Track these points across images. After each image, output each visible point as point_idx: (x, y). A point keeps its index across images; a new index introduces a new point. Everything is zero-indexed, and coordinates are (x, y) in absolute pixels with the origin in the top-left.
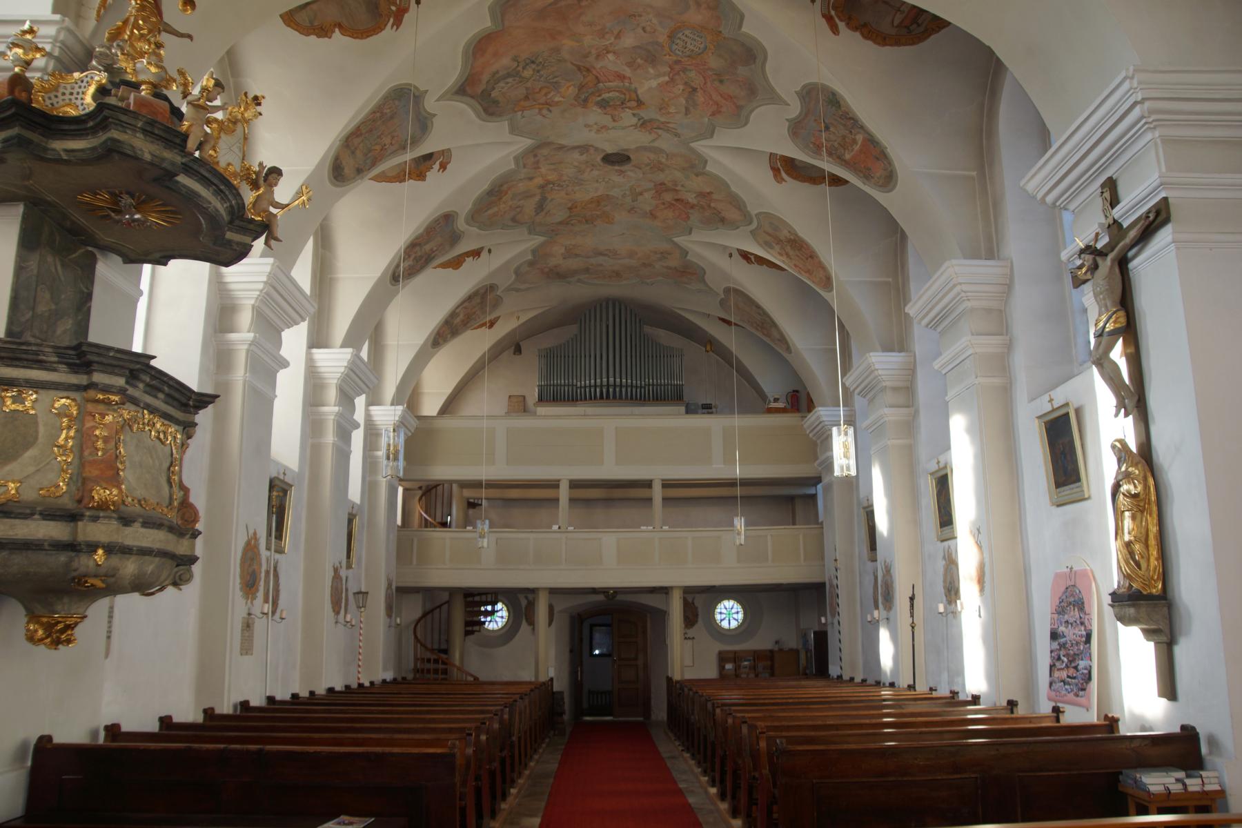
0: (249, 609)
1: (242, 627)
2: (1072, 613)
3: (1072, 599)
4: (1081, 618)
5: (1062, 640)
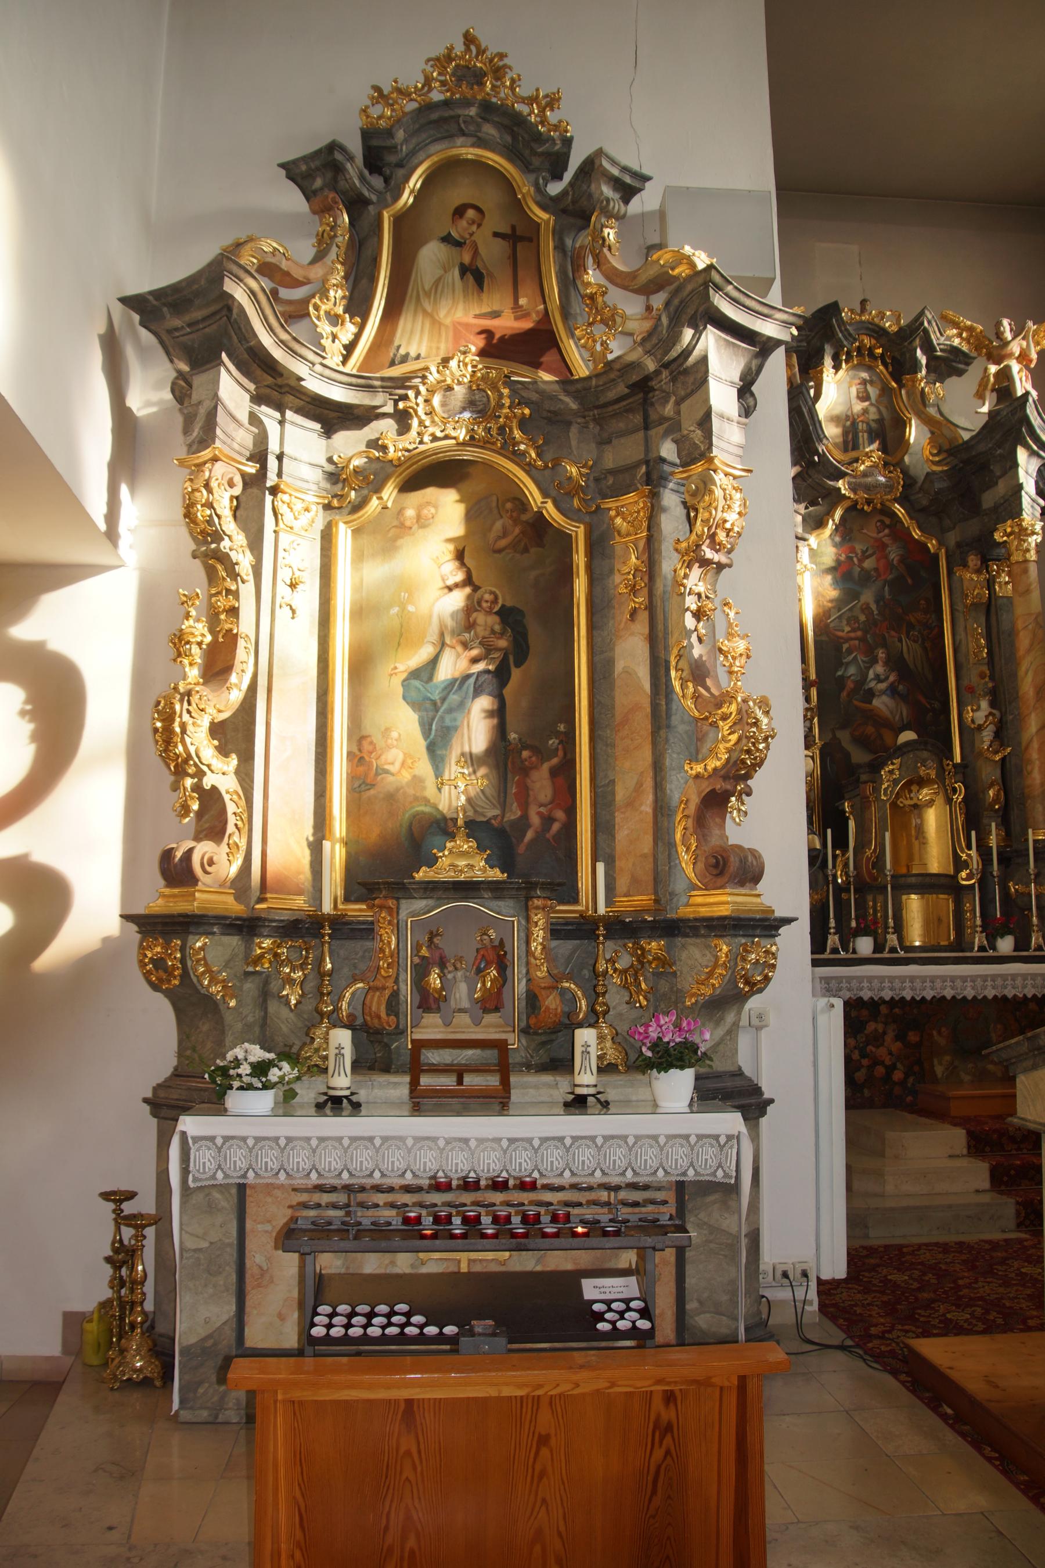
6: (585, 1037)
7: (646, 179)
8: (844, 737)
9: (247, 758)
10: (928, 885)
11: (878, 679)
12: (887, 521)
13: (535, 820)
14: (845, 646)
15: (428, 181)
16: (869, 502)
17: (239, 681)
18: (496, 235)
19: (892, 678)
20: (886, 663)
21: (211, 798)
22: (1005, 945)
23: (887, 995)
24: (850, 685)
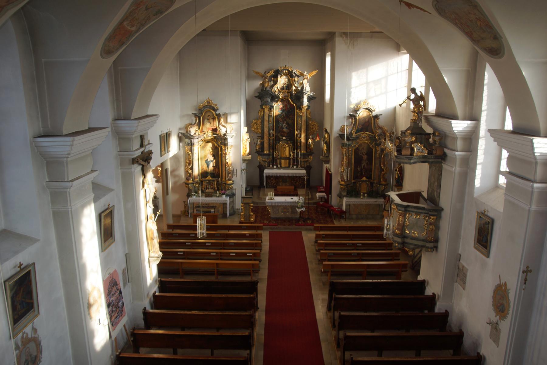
2: (114, 290)
4: (117, 288)
6: (218, 192)
7: (225, 113)
8: (279, 135)
10: (285, 159)
12: (288, 101)
13: (216, 172)
14: (280, 121)
15: (205, 113)
16: (285, 99)
17: (191, 164)
18: (212, 118)
19: (287, 126)
20: (286, 123)
21: (190, 174)
22: (295, 167)
23: (273, 175)
24: (280, 127)
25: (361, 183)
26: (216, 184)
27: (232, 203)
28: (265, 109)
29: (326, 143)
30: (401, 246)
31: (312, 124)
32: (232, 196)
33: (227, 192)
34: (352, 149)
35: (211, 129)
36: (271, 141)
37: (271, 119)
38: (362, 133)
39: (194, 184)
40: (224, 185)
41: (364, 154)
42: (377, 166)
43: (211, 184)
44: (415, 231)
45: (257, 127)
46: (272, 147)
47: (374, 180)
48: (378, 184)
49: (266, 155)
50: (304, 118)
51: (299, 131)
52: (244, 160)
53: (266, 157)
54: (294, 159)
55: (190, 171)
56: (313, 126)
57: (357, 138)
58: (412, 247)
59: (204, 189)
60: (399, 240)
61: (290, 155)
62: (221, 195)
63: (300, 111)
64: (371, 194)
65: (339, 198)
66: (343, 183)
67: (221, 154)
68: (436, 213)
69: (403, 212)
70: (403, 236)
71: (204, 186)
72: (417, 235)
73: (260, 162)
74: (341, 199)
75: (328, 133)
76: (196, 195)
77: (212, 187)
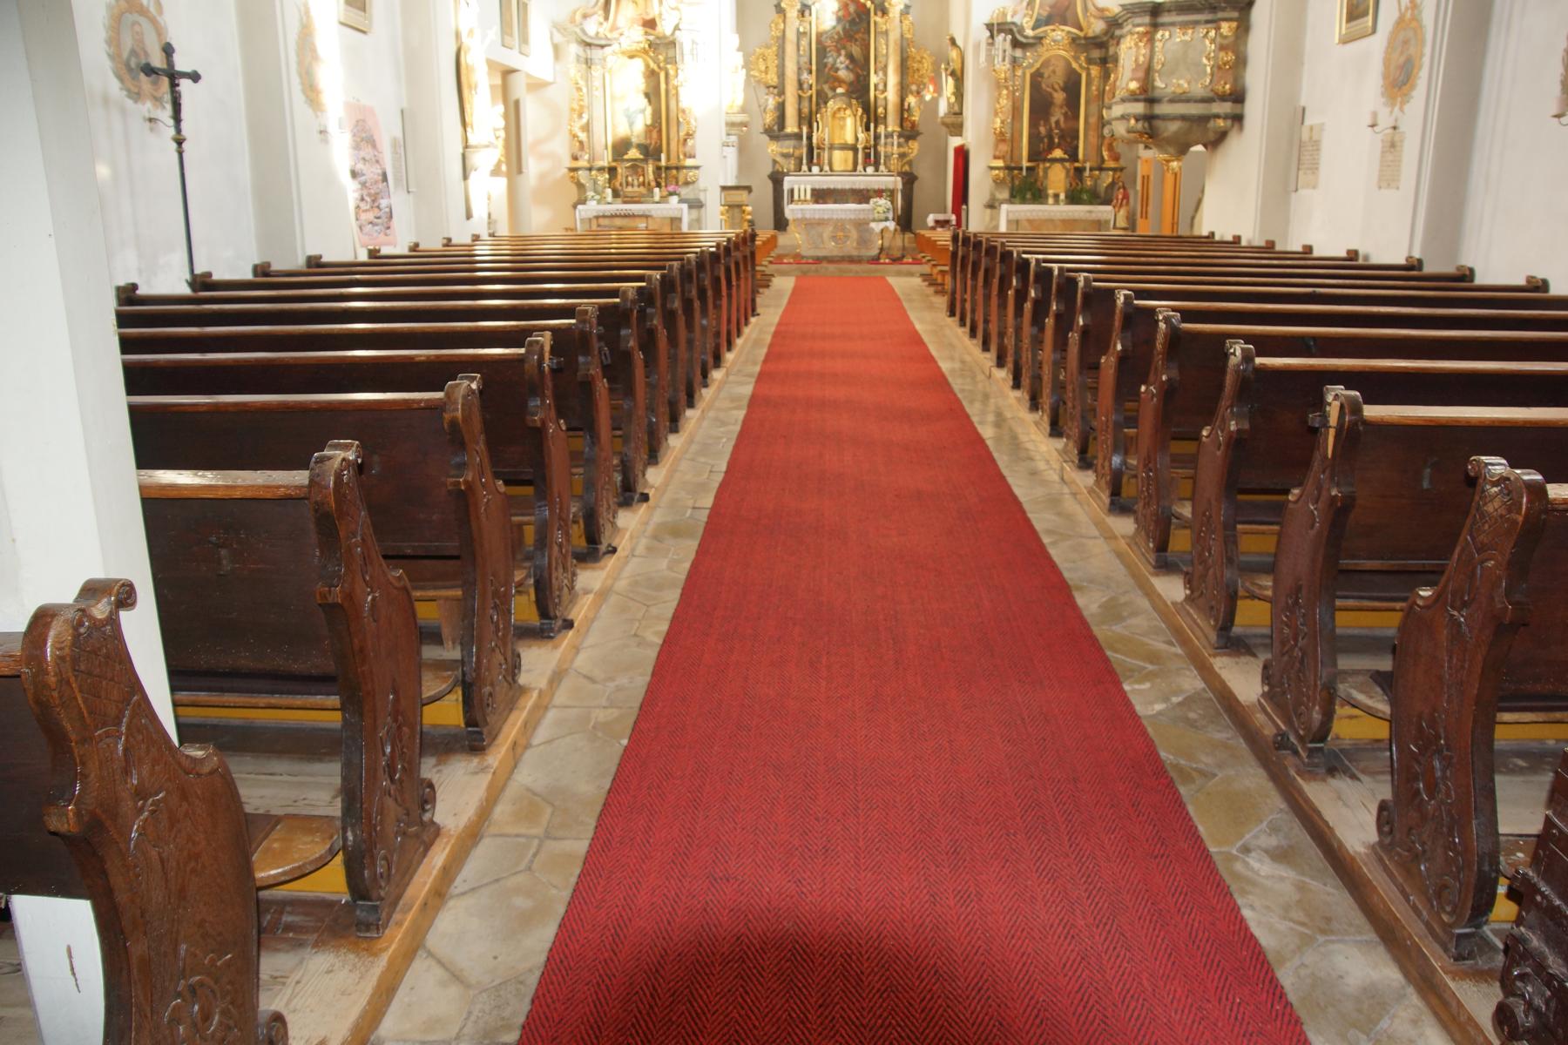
0: (1396, 120)
1: (1383, 147)
3: (364, 135)
5: (363, 179)
8: (826, 87)
9: (588, 131)
10: (844, 147)
11: (841, 63)
13: (653, 143)
17: (585, 116)
21: (581, 143)
22: (870, 170)
24: (829, 66)
25: (1048, 165)
26: (654, 173)
27: (698, 222)
28: (788, 10)
29: (953, 74)
30: (1144, 127)
31: (918, 58)
32: (696, 205)
33: (684, 191)
34: (1024, 74)
35: (641, 22)
36: (805, 104)
37: (804, 42)
38: (1052, 27)
39: (594, 172)
40: (674, 172)
41: (1056, 87)
42: (1093, 120)
43: (640, 170)
44: (1178, 79)
45: (767, 67)
46: (808, 119)
47: (1085, 162)
48: (1096, 169)
49: (789, 136)
50: (894, 36)
51: (881, 74)
52: (731, 125)
53: (792, 143)
54: (867, 151)
55: (583, 136)
56: (920, 62)
57: (1039, 39)
58: (1173, 127)
59: (621, 185)
60: (1139, 108)
61: (857, 139)
62: (664, 199)
63: (883, 16)
64: (1073, 198)
65: (988, 211)
66: (1000, 163)
67: (667, 91)
68: (1235, 14)
69: (1148, 29)
70: (1147, 95)
71: (619, 177)
72: (1186, 85)
73: (775, 162)
74: (994, 211)
75: (958, 47)
76: (598, 197)
77: (641, 179)
